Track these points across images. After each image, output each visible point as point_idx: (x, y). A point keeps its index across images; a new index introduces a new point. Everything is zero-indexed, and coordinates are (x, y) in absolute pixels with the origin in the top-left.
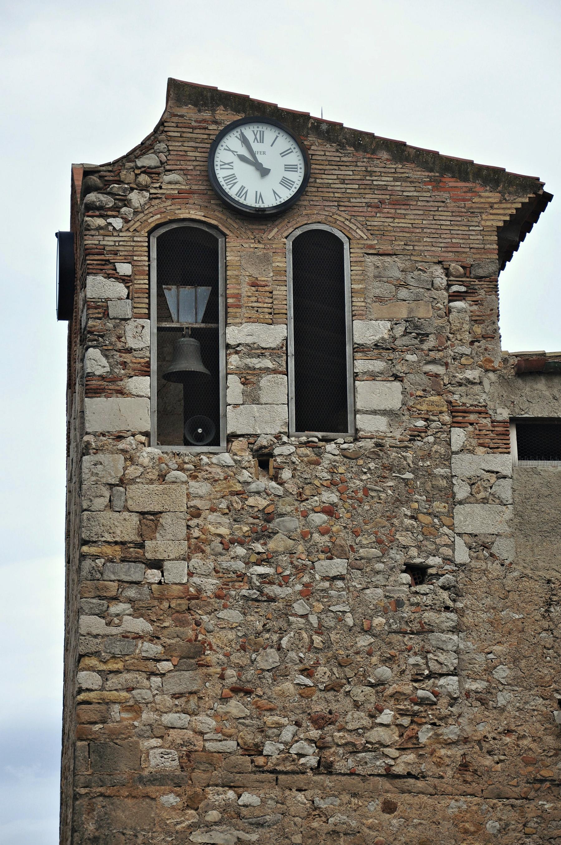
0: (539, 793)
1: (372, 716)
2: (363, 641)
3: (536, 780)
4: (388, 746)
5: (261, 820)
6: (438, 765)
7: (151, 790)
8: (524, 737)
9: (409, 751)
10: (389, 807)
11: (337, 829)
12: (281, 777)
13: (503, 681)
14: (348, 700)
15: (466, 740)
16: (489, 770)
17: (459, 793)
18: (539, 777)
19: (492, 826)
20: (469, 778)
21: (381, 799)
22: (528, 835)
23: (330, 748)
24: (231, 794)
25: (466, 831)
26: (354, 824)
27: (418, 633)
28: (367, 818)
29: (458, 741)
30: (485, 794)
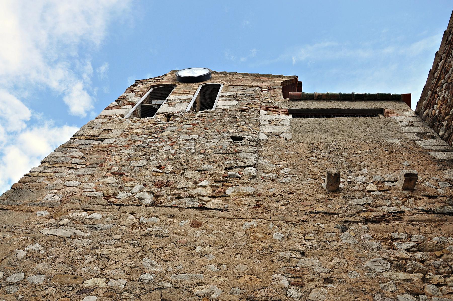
0: (315, 219)
1: (196, 183)
2: (198, 157)
3: (312, 213)
4: (203, 196)
5: (96, 226)
6: (238, 205)
7: (33, 208)
8: (302, 194)
9: (217, 199)
10: (195, 224)
11: (151, 233)
12: (122, 208)
13: (287, 173)
14: (182, 177)
15: (260, 194)
16: (276, 209)
17: (252, 217)
18: (314, 211)
19: (276, 236)
20: (260, 211)
21: (191, 219)
22: (307, 240)
23: (163, 196)
24: (84, 214)
25: (256, 238)
26: (166, 232)
27: (233, 153)
28: (177, 229)
29: (254, 194)
30: (272, 219)
